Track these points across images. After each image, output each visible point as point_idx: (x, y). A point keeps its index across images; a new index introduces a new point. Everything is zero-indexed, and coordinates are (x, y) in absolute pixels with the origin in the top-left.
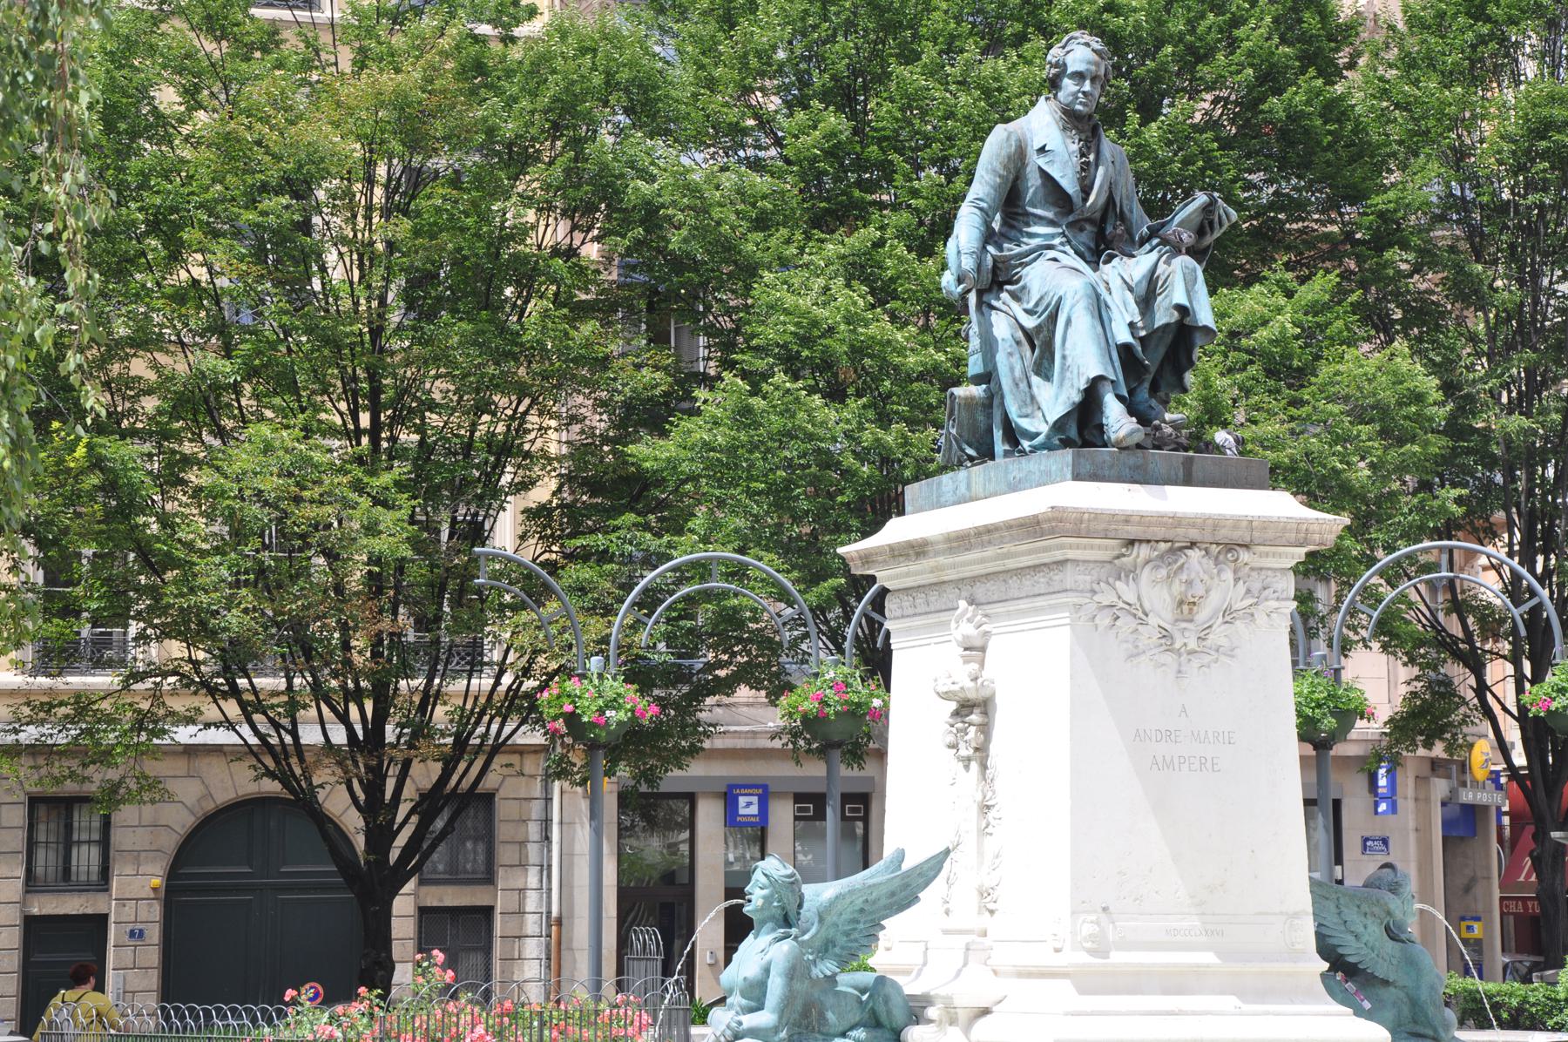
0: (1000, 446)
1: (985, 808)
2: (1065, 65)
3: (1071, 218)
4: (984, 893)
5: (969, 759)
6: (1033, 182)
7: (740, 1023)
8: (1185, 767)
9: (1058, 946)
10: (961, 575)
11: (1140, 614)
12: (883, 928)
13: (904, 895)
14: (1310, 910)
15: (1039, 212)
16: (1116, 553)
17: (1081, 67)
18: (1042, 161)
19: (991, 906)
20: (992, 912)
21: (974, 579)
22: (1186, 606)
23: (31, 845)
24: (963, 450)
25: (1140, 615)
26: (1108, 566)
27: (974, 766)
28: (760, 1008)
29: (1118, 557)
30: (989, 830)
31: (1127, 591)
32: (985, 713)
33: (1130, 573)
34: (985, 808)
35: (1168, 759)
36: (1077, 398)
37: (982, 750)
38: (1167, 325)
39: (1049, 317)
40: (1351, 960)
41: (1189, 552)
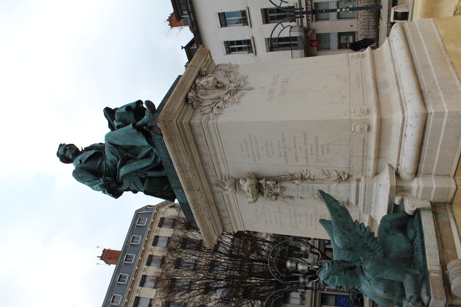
0: (163, 173)
1: (303, 178)
2: (62, 155)
4: (340, 179)
5: (281, 187)
6: (89, 165)
7: (411, 297)
9: (366, 127)
10: (209, 191)
12: (357, 221)
13: (339, 213)
15: (99, 162)
16: (190, 106)
18: (83, 161)
19: (346, 177)
20: (349, 176)
21: (210, 184)
22: (218, 86)
24: (166, 190)
26: (196, 111)
27: (284, 184)
28: (402, 285)
29: (193, 106)
30: (312, 177)
32: (261, 179)
33: (200, 102)
34: (303, 178)
37: (277, 180)
38: (134, 116)
39: (116, 148)
41: (197, 82)
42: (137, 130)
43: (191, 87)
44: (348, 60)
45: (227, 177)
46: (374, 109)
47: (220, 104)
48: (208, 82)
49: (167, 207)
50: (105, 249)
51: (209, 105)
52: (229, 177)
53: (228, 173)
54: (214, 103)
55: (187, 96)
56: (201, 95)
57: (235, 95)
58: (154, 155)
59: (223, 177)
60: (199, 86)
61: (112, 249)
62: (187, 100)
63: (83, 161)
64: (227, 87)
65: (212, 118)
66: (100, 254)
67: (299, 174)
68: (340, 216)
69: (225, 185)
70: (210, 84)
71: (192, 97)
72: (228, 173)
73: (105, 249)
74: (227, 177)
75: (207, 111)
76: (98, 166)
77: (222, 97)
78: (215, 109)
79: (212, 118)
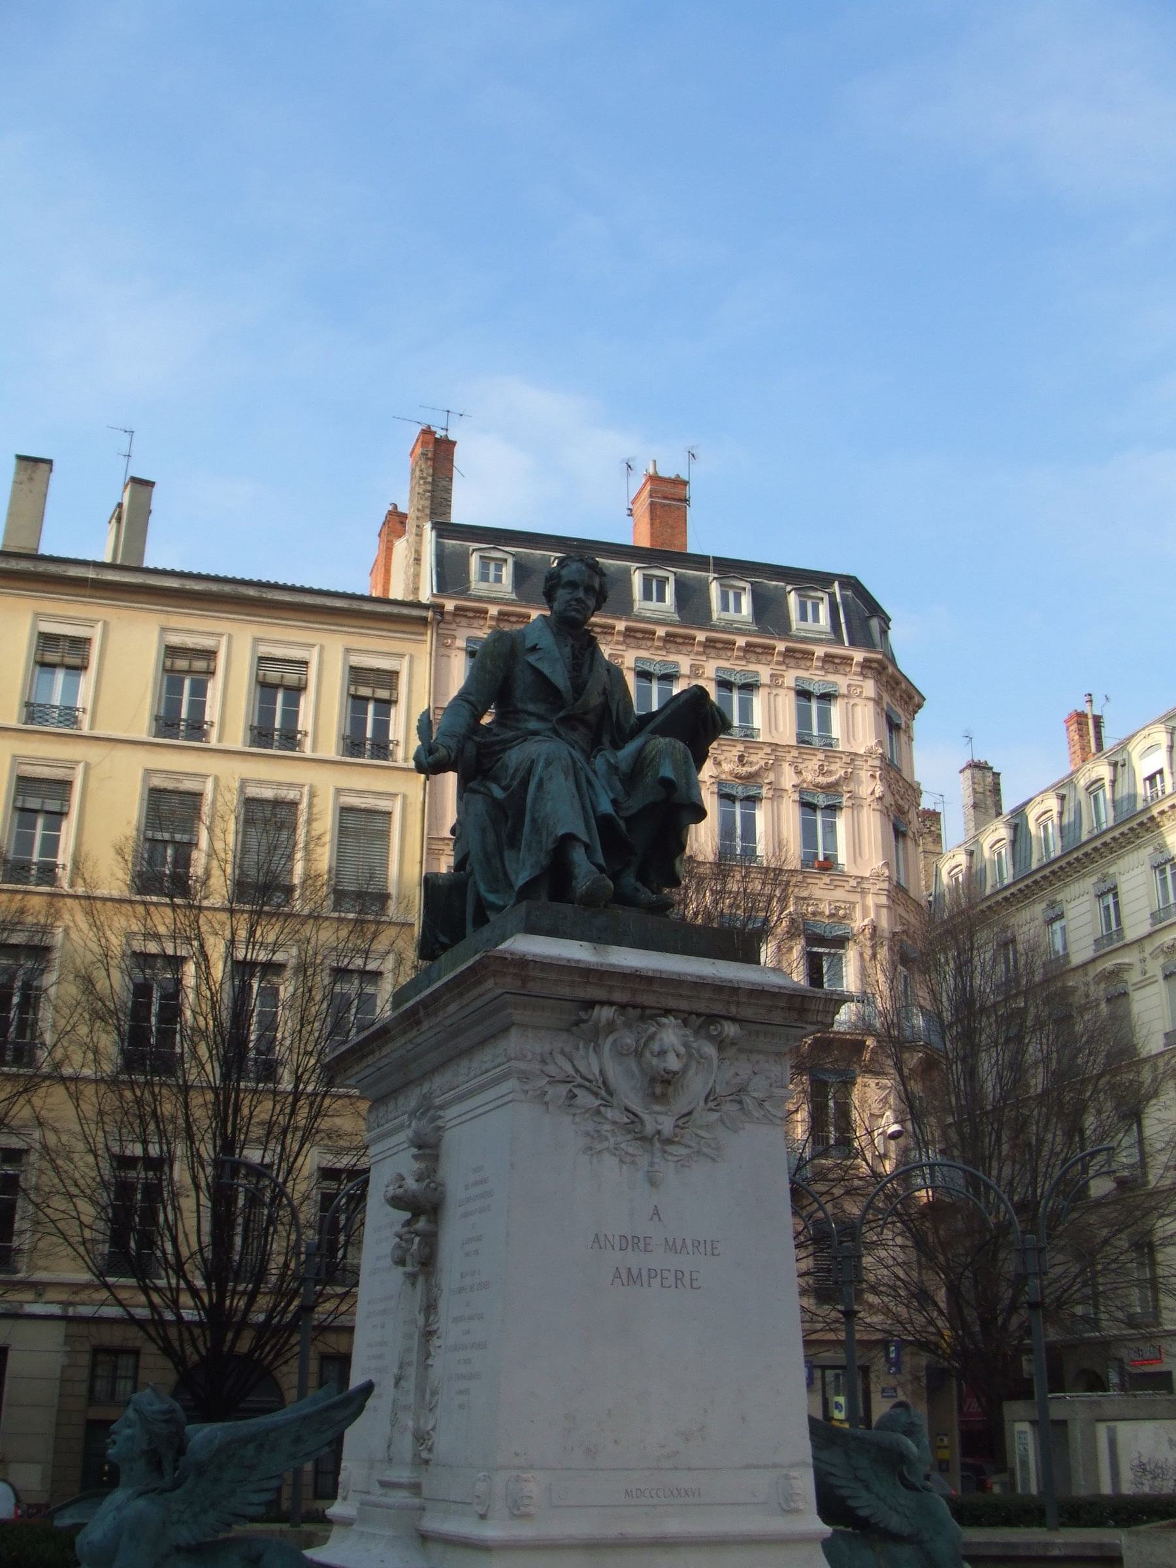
3: (561, 714)
4: (421, 1438)
6: (523, 679)
8: (656, 1283)
11: (603, 1093)
14: (810, 1460)
15: (531, 707)
17: (575, 577)
18: (531, 659)
19: (425, 1455)
20: (427, 1462)
22: (661, 1085)
23: (93, 1377)
25: (605, 1090)
26: (565, 1036)
29: (577, 1023)
30: (430, 1362)
31: (590, 1064)
35: (635, 1272)
36: (544, 861)
40: (862, 1513)
41: (664, 1020)
42: (554, 850)
43: (643, 1008)
44: (775, 1466)
45: (440, 1123)
46: (525, 1531)
47: (586, 1099)
48: (662, 1053)
49: (886, 698)
50: (685, 483)
51: (577, 1071)
52: (440, 1128)
53: (449, 1125)
54: (587, 1080)
55: (602, 1003)
56: (615, 1041)
57: (629, 1137)
58: (501, 903)
59: (441, 1113)
60: (647, 1029)
61: (691, 512)
62: (590, 1005)
63: (531, 659)
64: (657, 1108)
65: (526, 1087)
66: (666, 472)
67: (434, 1327)
68: (298, 1440)
69: (420, 1119)
70: (655, 1061)
71: (598, 1021)
72: (449, 1125)
73: (685, 483)
74: (440, 1123)
75: (551, 1069)
76: (520, 705)
77: (615, 1101)
78: (563, 1089)
79: (526, 1087)
